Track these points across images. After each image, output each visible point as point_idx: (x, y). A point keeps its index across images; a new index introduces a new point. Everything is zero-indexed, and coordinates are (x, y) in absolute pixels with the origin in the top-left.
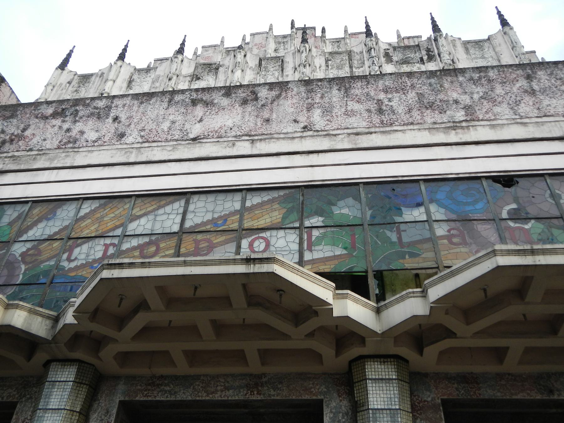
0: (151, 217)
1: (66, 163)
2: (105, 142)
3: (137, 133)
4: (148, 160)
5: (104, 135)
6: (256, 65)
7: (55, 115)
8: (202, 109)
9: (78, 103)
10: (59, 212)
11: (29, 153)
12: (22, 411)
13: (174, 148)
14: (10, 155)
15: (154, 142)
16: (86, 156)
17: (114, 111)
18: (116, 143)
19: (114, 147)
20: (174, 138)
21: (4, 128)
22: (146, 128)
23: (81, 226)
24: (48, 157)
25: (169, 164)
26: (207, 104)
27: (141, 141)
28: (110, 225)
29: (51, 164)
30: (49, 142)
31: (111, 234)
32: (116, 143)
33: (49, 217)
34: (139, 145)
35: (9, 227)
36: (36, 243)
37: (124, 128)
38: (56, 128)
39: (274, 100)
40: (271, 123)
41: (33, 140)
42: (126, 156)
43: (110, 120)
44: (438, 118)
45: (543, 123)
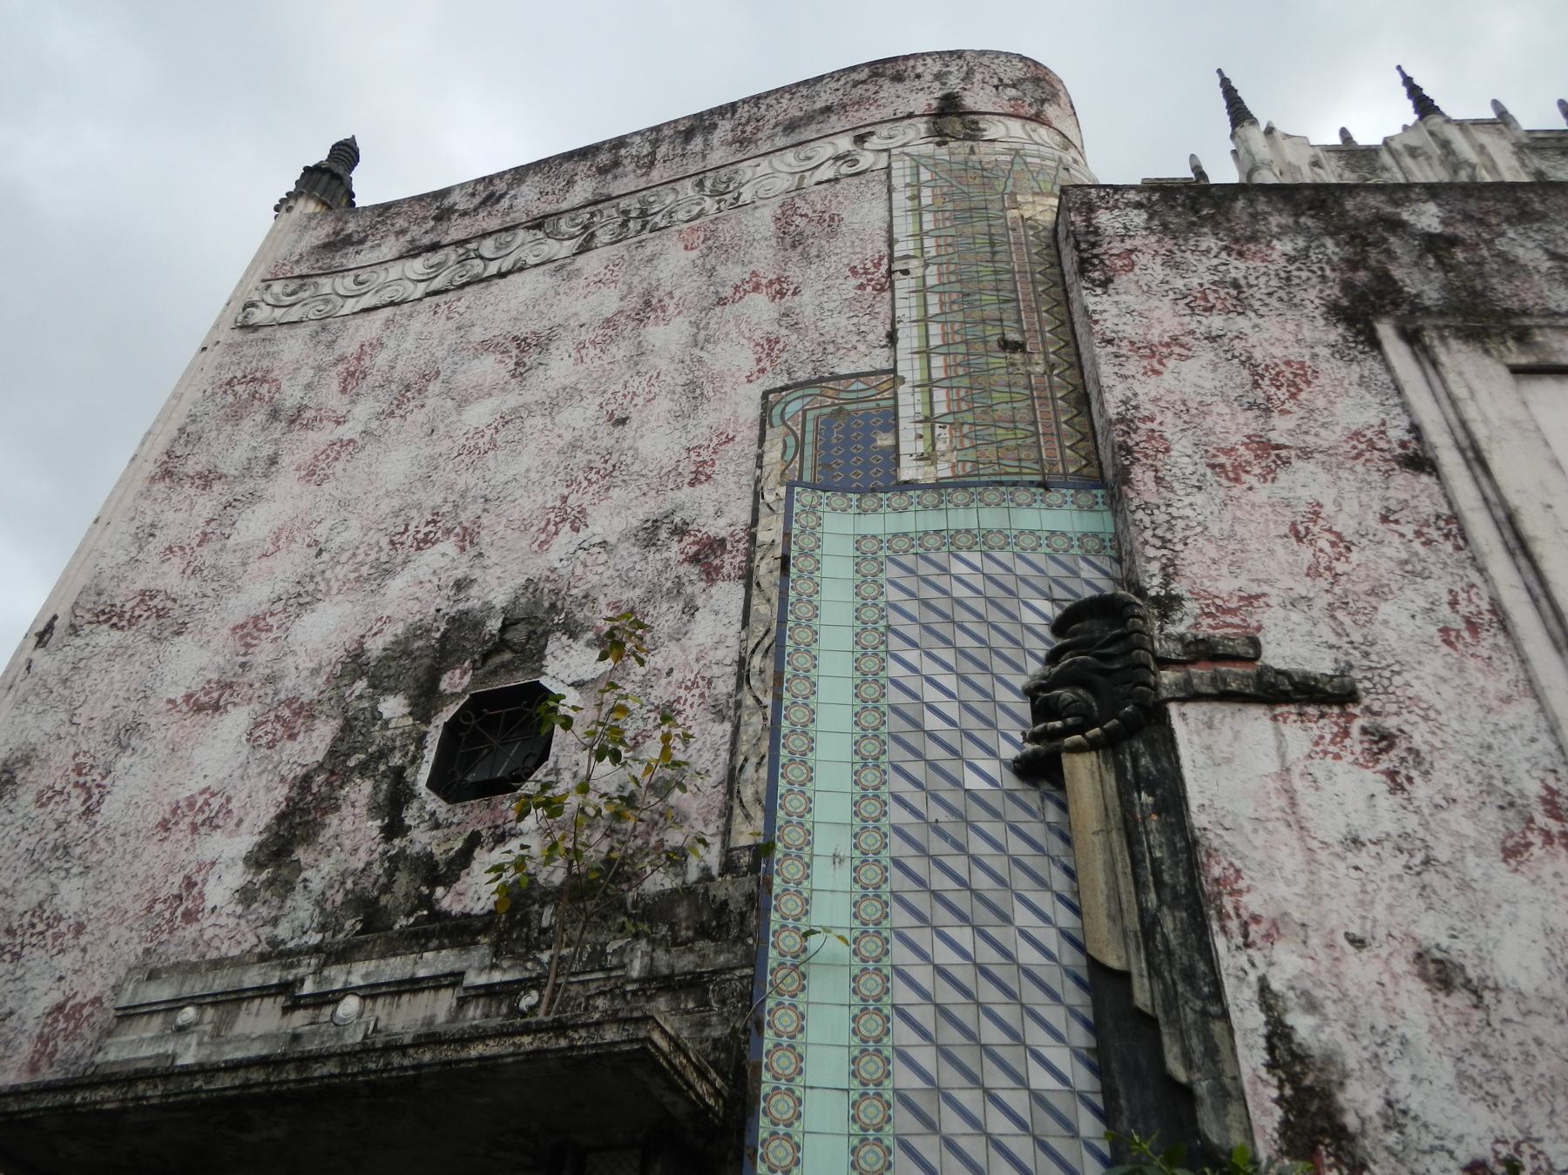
21: (1550, 247)
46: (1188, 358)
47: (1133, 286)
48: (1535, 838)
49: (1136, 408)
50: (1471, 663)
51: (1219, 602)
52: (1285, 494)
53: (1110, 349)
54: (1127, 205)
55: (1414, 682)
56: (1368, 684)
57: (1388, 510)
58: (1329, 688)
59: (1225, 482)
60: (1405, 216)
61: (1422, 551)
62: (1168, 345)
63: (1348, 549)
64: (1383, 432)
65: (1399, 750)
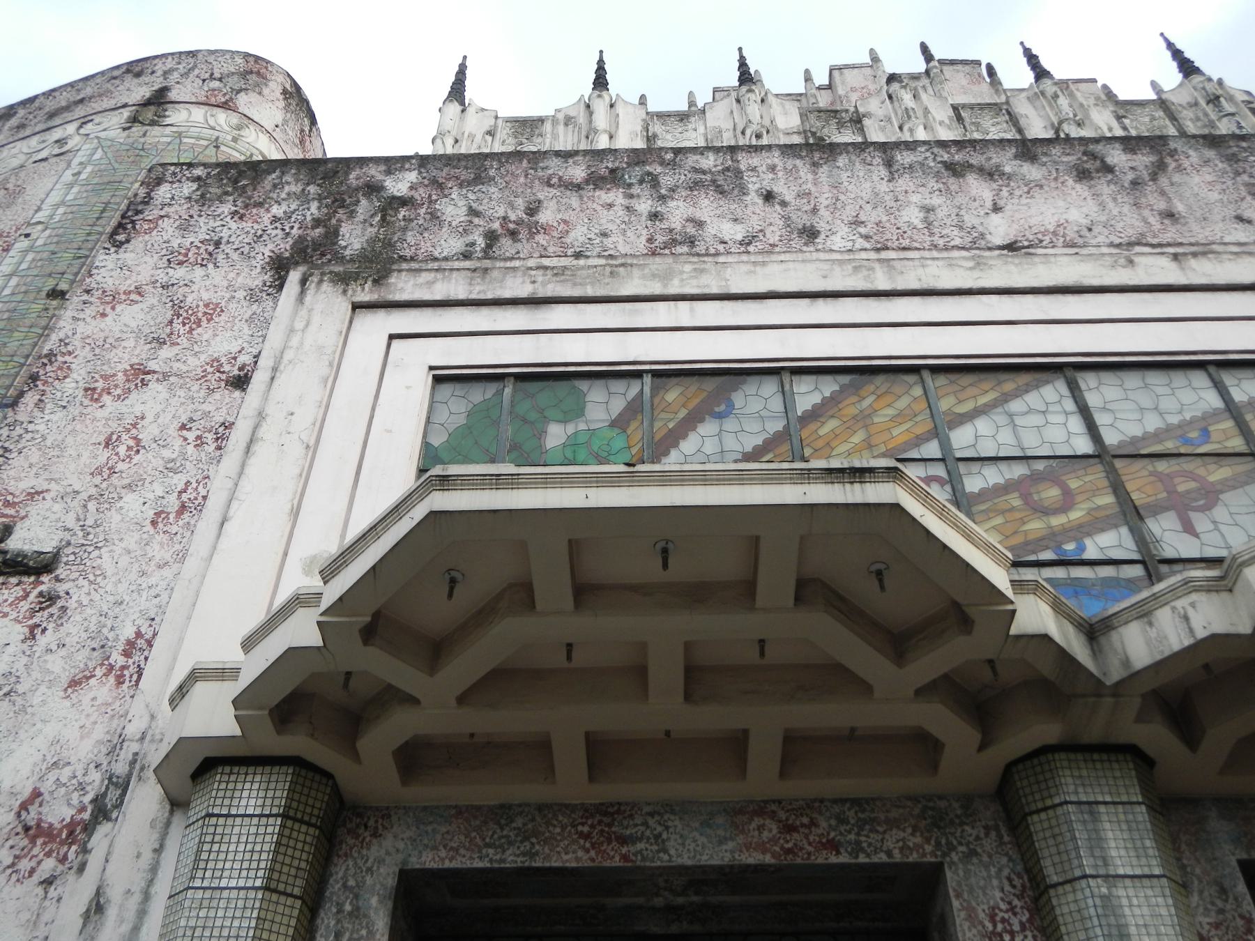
0: (999, 417)
1: (707, 286)
2: (773, 245)
3: (846, 229)
4: (925, 286)
6: (950, 118)
7: (596, 181)
8: (985, 185)
9: (642, 158)
10: (738, 399)
11: (582, 262)
12: (971, 891)
14: (531, 263)
16: (754, 272)
17: (754, 179)
18: (805, 248)
20: (952, 243)
21: (474, 205)
22: (862, 218)
23: (822, 432)
24: (647, 271)
25: (984, 298)
26: (990, 174)
27: (868, 246)
29: (665, 286)
30: (621, 241)
33: (717, 409)
34: (873, 255)
35: (617, 431)
37: (805, 217)
39: (1156, 174)
40: (1182, 220)
41: (572, 235)
42: (860, 275)
43: (753, 198)
46: (137, 302)
47: (141, 245)
48: (99, 672)
49: (66, 344)
50: (161, 537)
51: (9, 498)
52: (124, 410)
53: (85, 297)
54: (188, 179)
55: (106, 556)
56: (72, 558)
57: (192, 420)
58: (31, 563)
59: (86, 402)
60: (386, 184)
61: (190, 449)
62: (130, 292)
63: (138, 451)
64: (235, 358)
65: (54, 610)
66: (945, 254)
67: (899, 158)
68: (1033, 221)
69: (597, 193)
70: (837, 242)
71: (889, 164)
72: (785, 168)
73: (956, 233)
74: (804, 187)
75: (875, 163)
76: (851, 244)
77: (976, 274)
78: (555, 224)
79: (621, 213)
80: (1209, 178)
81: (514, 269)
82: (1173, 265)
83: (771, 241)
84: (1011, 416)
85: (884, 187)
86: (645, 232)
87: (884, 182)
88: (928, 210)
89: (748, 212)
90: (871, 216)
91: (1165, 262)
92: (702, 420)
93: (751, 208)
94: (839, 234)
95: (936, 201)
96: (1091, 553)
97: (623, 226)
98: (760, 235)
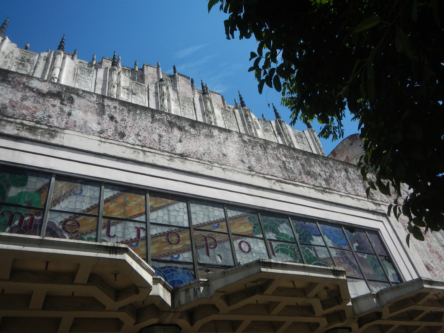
0: (165, 211)
5: (107, 130)
7: (51, 94)
11: (39, 126)
13: (171, 159)
14: (18, 121)
15: (151, 148)
17: (108, 110)
18: (119, 140)
19: (120, 143)
20: (165, 150)
22: (140, 134)
26: (181, 129)
27: (140, 144)
28: (136, 212)
30: (56, 121)
31: (137, 219)
32: (119, 140)
34: (140, 148)
36: (72, 215)
38: (57, 109)
41: (37, 113)
42: (135, 155)
43: (106, 117)
44: (314, 182)
45: (360, 200)
66: (162, 153)
67: (156, 116)
68: (190, 148)
69: (51, 100)
70: (131, 140)
71: (153, 117)
72: (119, 109)
73: (167, 146)
74: (124, 117)
75: (148, 115)
76: (134, 142)
77: (170, 162)
78: (32, 107)
79: (58, 110)
80: (238, 146)
81: (11, 122)
82: (222, 172)
83: (109, 135)
84: (169, 211)
85: (149, 124)
86: (65, 119)
87: (150, 123)
88: (160, 136)
89: (103, 122)
90: (144, 134)
91: (220, 170)
92: (70, 195)
93: (105, 120)
94: (132, 138)
95: (163, 134)
96: (181, 259)
97: (58, 115)
98: (106, 131)
